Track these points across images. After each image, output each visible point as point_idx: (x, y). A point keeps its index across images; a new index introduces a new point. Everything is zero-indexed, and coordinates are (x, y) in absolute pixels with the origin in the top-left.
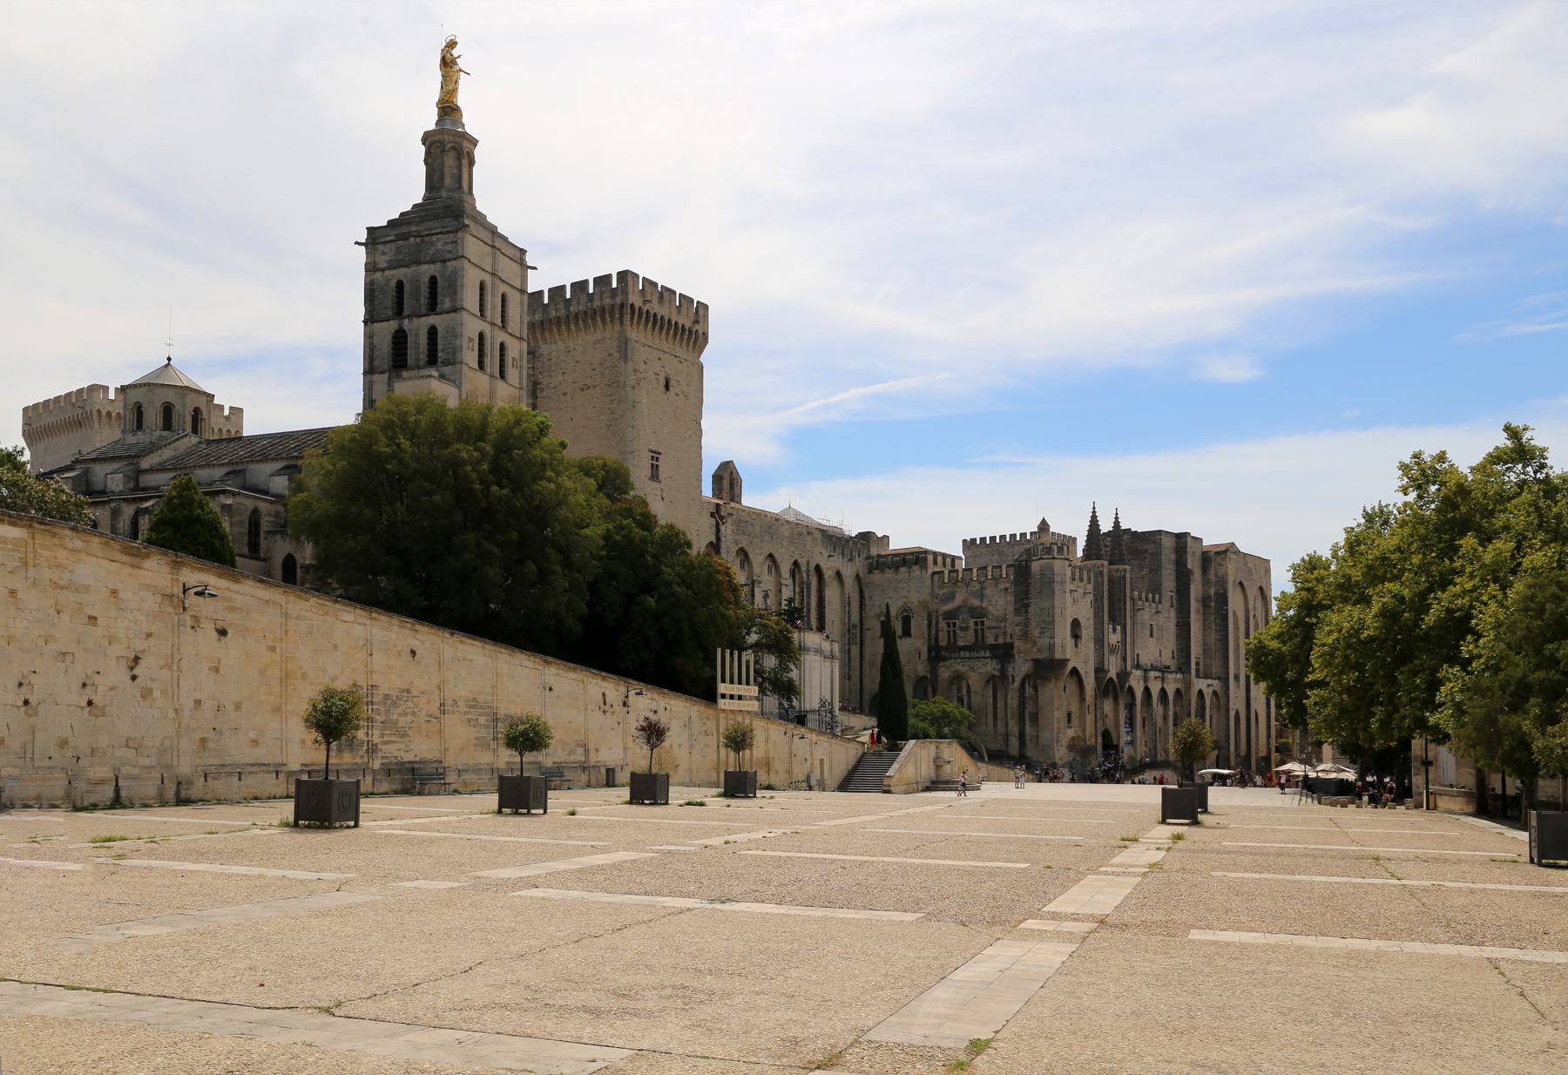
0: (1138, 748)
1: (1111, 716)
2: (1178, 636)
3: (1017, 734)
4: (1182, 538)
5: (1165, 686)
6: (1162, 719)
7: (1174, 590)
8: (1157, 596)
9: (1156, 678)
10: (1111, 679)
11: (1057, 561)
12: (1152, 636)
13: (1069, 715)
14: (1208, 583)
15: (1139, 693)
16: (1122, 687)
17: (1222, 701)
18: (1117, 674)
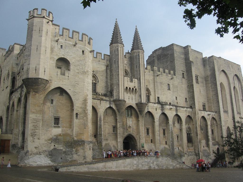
0: (157, 145)
1: (135, 127)
2: (189, 92)
3: (21, 133)
4: (187, 48)
5: (179, 114)
6: (179, 130)
7: (185, 71)
8: (172, 72)
9: (171, 109)
10: (130, 107)
11: (35, 19)
12: (169, 89)
14: (206, 71)
15: (157, 115)
16: (141, 111)
17: (218, 122)
18: (136, 104)
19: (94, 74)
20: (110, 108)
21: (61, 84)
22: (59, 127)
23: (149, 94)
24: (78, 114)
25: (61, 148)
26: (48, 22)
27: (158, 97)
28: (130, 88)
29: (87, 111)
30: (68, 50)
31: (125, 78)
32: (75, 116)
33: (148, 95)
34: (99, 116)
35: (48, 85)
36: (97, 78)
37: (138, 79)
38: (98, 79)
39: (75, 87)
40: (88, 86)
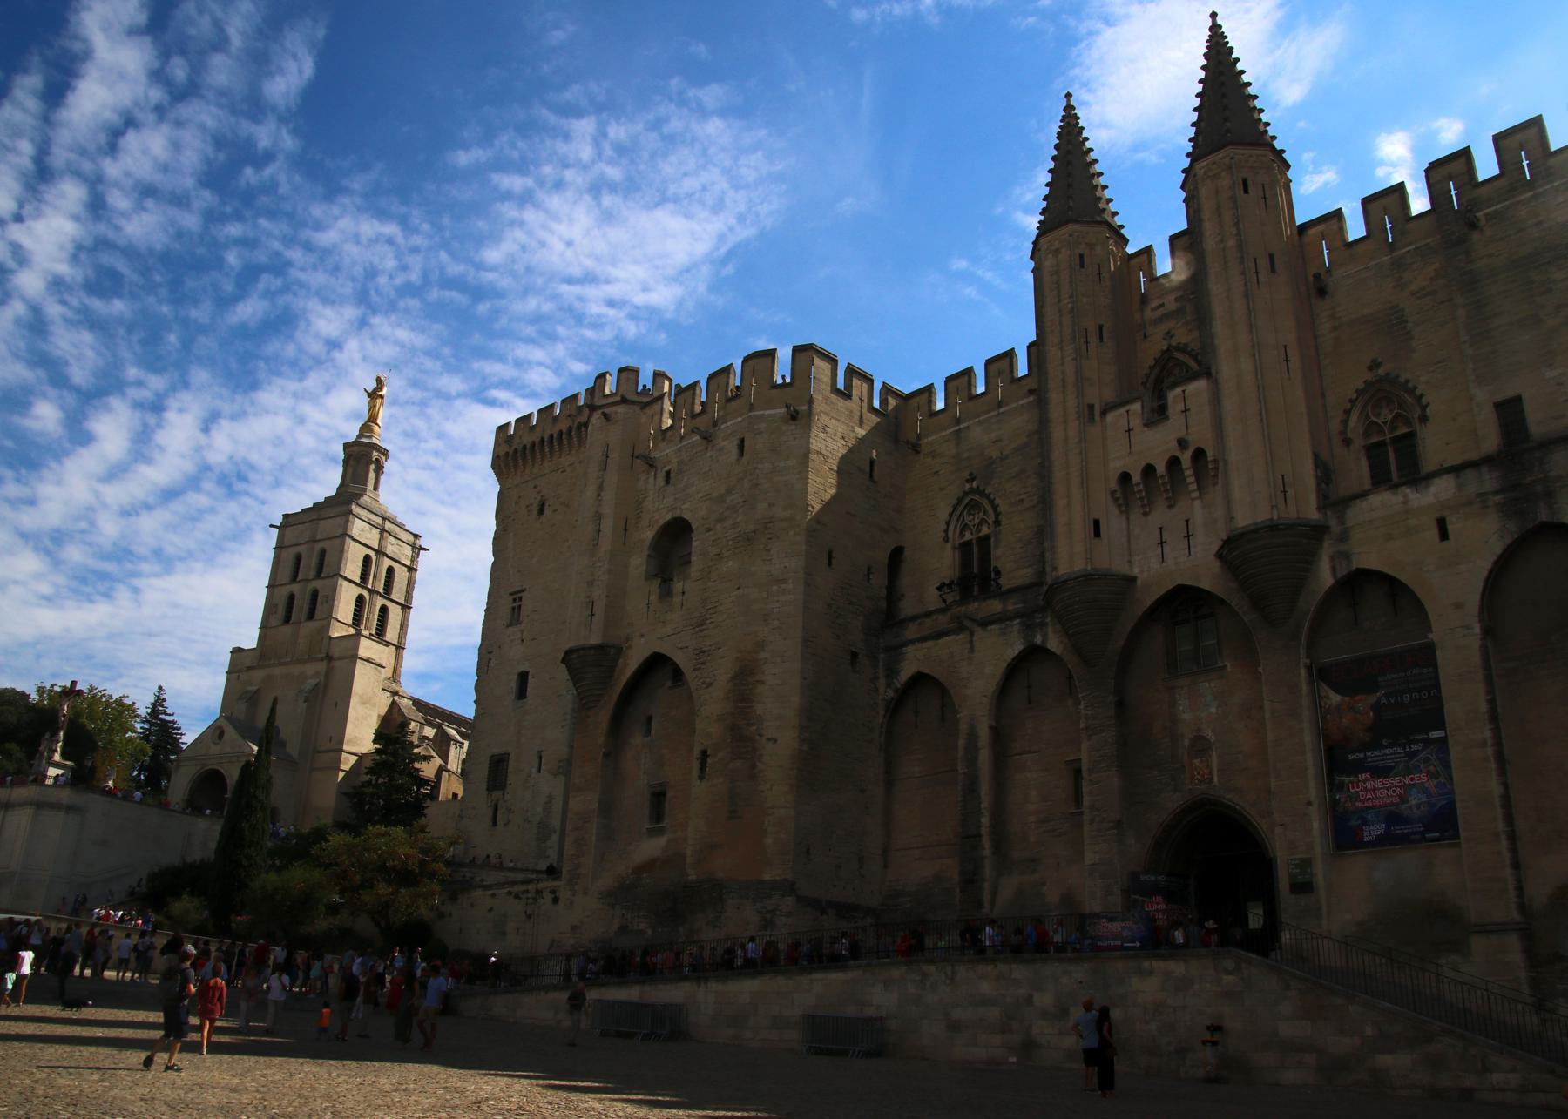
13: (658, 797)
18: (1219, 555)
19: (977, 491)
20: (1033, 654)
21: (659, 636)
22: (661, 831)
23: (1408, 423)
24: (708, 753)
25: (642, 926)
26: (605, 416)
27: (1499, 406)
28: (1149, 470)
29: (753, 728)
30: (686, 479)
31: (1110, 417)
32: (696, 765)
33: (1402, 430)
34: (963, 727)
35: (621, 660)
36: (992, 502)
37: (1207, 372)
38: (995, 508)
39: (704, 627)
40: (765, 595)
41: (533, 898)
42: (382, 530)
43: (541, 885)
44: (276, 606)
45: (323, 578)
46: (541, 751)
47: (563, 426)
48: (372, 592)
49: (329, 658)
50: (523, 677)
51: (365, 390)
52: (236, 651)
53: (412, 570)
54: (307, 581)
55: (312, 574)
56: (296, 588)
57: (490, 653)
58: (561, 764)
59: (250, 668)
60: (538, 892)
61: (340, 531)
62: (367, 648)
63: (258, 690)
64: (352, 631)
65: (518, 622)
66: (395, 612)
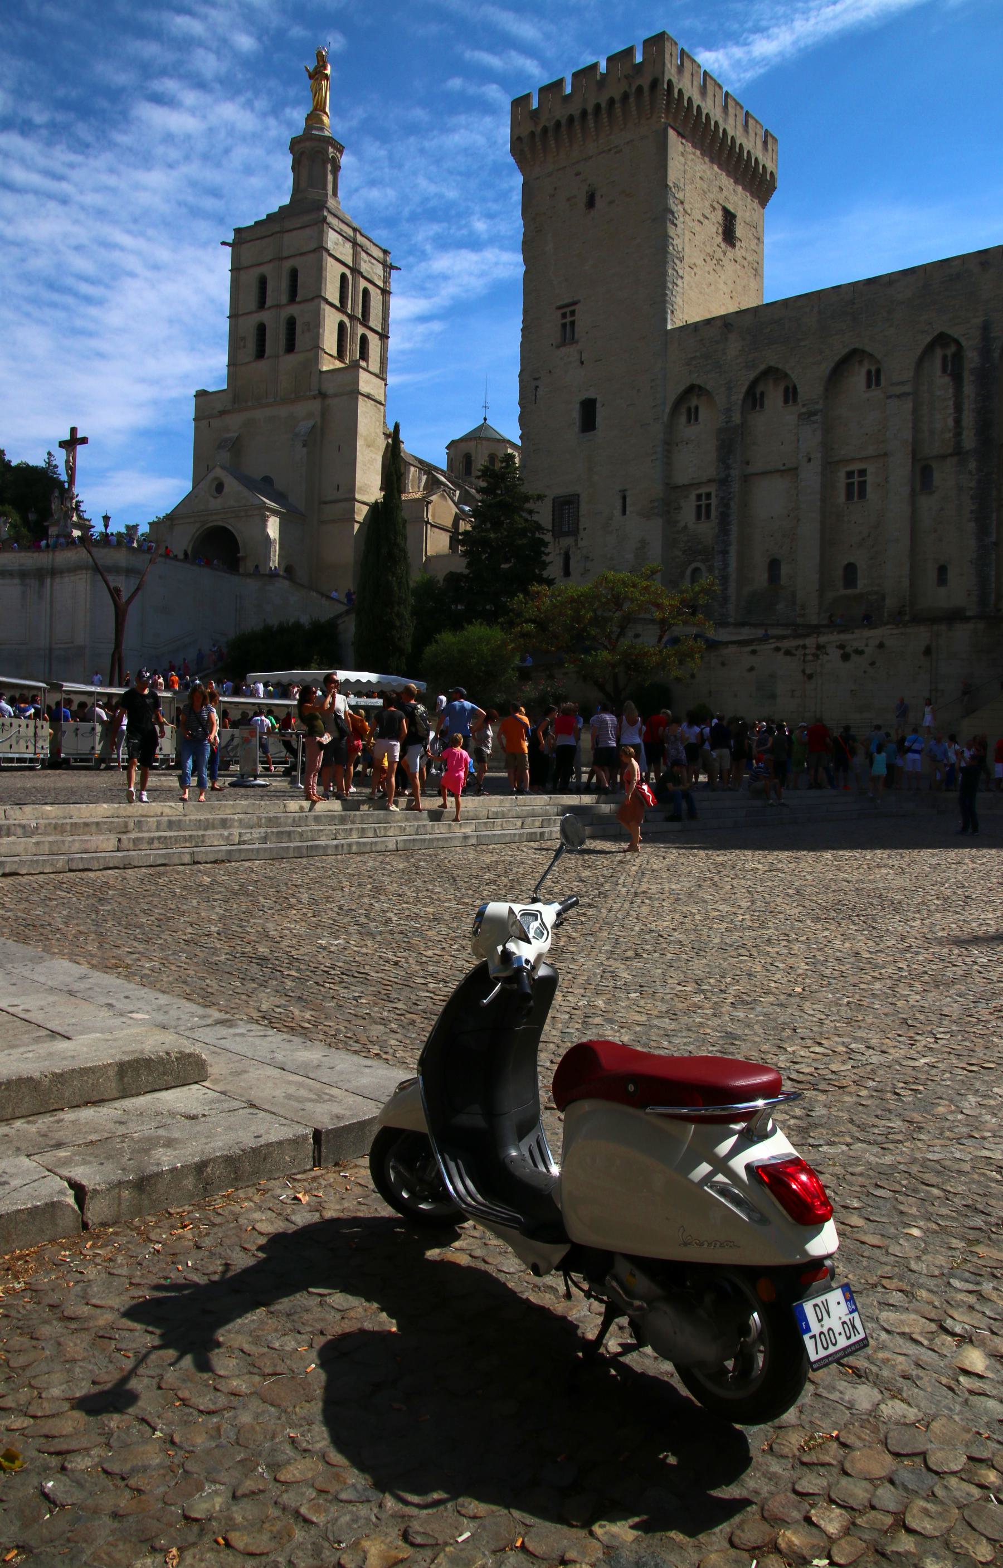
41: (814, 655)
42: (355, 244)
43: (823, 639)
44: (243, 339)
45: (299, 303)
46: (624, 491)
47: (615, 91)
48: (351, 317)
49: (322, 395)
50: (589, 408)
51: (307, 70)
52: (201, 395)
53: (385, 292)
54: (278, 306)
55: (284, 299)
56: (265, 316)
57: (536, 379)
58: (656, 504)
59: (222, 413)
60: (819, 647)
61: (313, 246)
62: (367, 383)
63: (238, 438)
64: (339, 365)
65: (573, 341)
66: (374, 341)
